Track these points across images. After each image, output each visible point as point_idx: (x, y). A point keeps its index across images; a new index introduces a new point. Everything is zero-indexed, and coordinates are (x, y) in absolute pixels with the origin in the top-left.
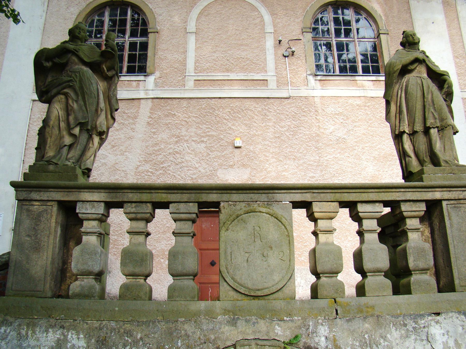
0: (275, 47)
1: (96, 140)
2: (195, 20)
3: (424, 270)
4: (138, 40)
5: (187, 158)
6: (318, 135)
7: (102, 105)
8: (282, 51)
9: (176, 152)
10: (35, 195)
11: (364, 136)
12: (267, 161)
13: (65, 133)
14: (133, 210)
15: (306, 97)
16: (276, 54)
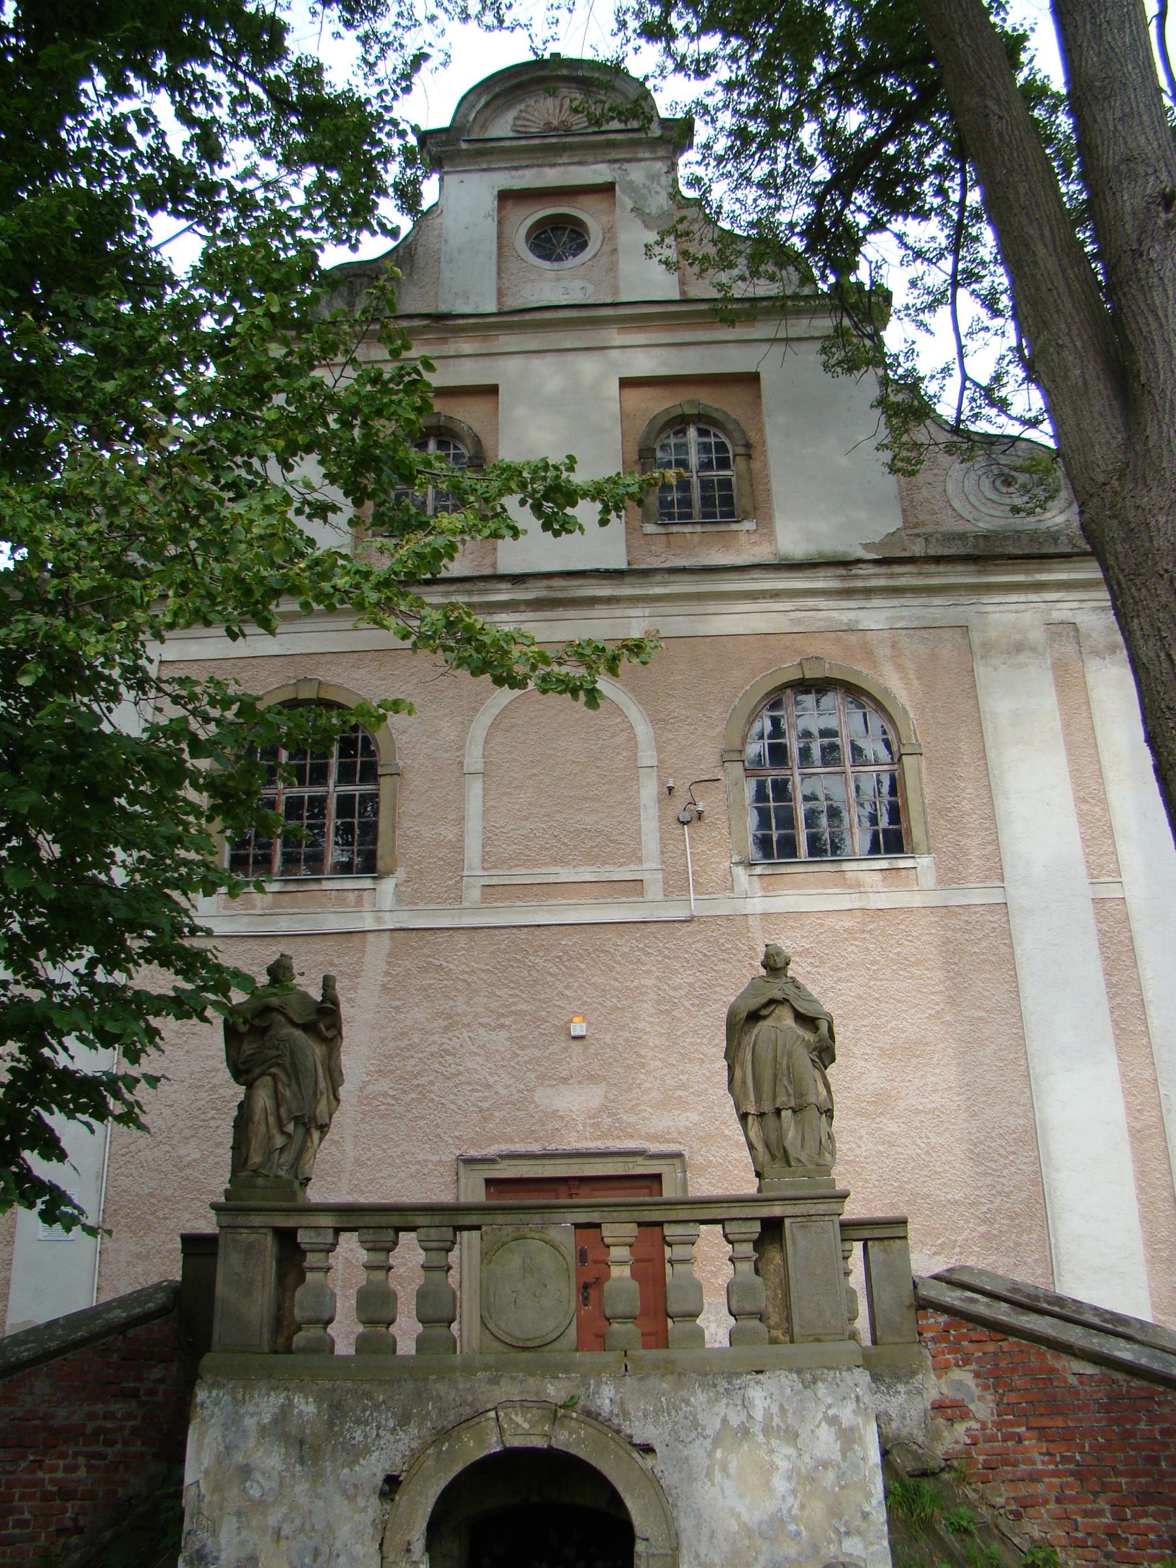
0: (660, 801)
1: (316, 1135)
2: (481, 741)
3: (626, 1318)
4: (357, 789)
5: (469, 1065)
7: (322, 1084)
8: (678, 807)
9: (445, 1051)
10: (241, 1220)
11: (859, 1002)
12: (643, 1066)
13: (275, 1131)
14: (370, 1238)
15: (728, 918)
16: (662, 819)
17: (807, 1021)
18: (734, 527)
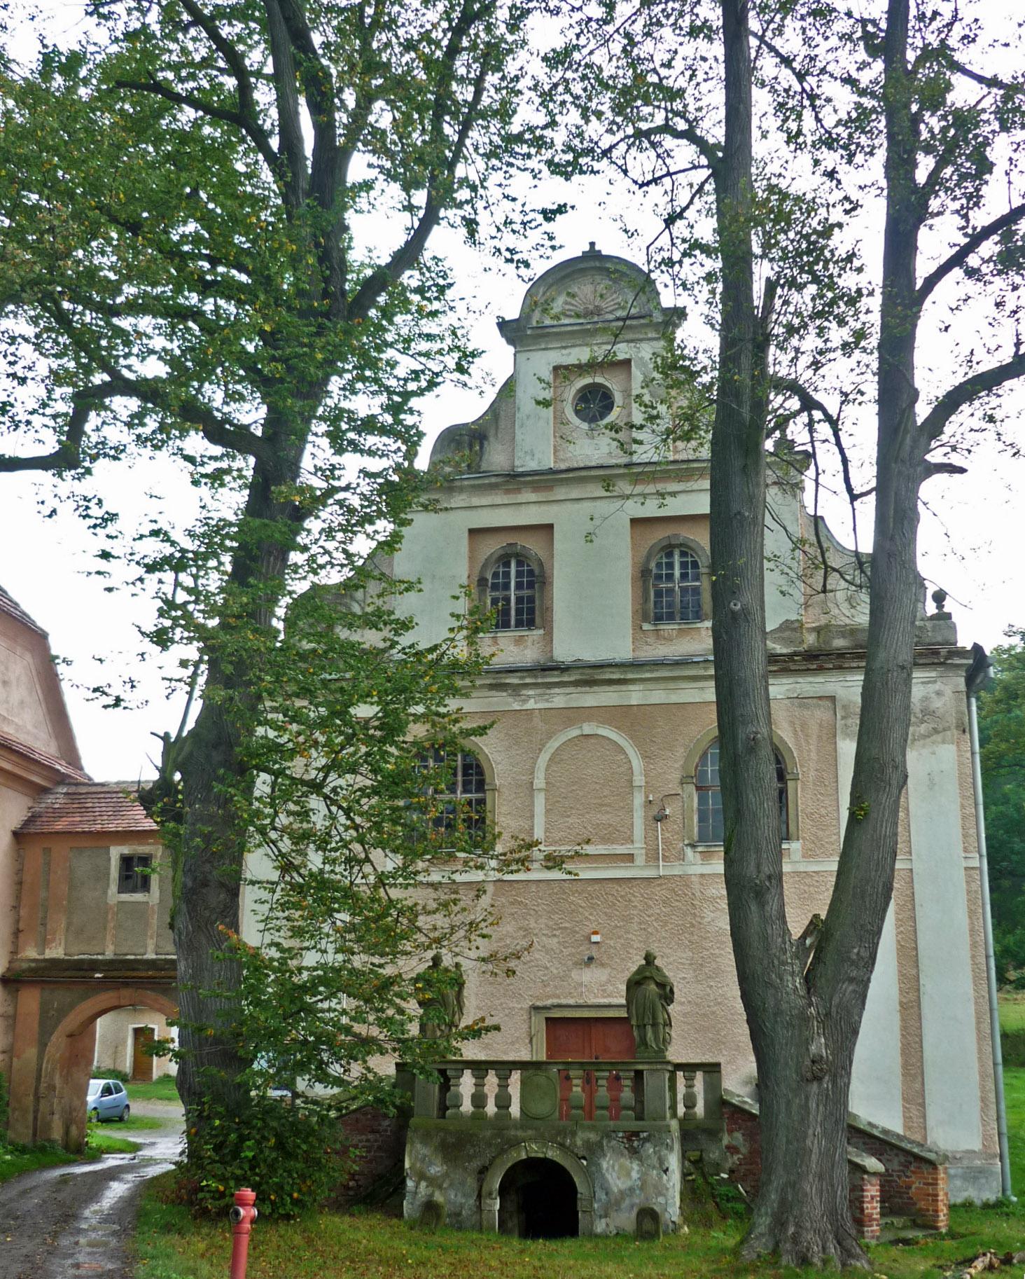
2: (543, 769)
6: (693, 926)
8: (655, 811)
16: (646, 818)
17: (662, 985)
18: (699, 625)
